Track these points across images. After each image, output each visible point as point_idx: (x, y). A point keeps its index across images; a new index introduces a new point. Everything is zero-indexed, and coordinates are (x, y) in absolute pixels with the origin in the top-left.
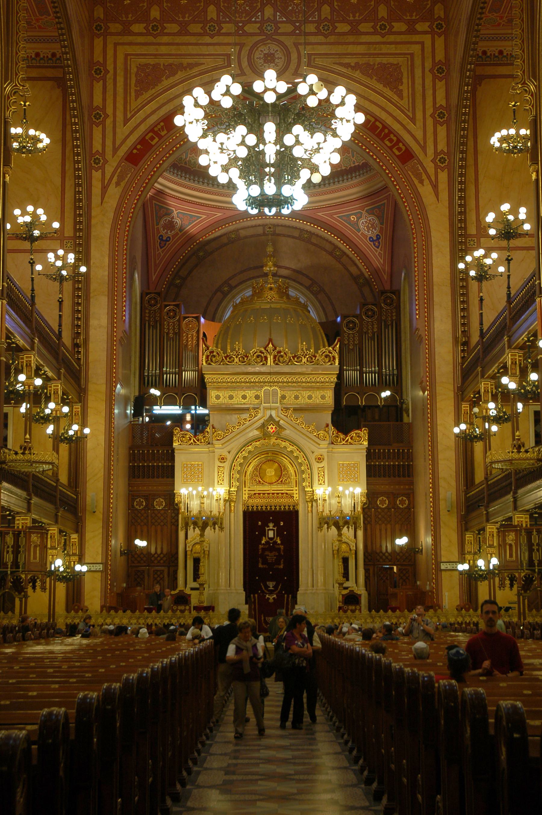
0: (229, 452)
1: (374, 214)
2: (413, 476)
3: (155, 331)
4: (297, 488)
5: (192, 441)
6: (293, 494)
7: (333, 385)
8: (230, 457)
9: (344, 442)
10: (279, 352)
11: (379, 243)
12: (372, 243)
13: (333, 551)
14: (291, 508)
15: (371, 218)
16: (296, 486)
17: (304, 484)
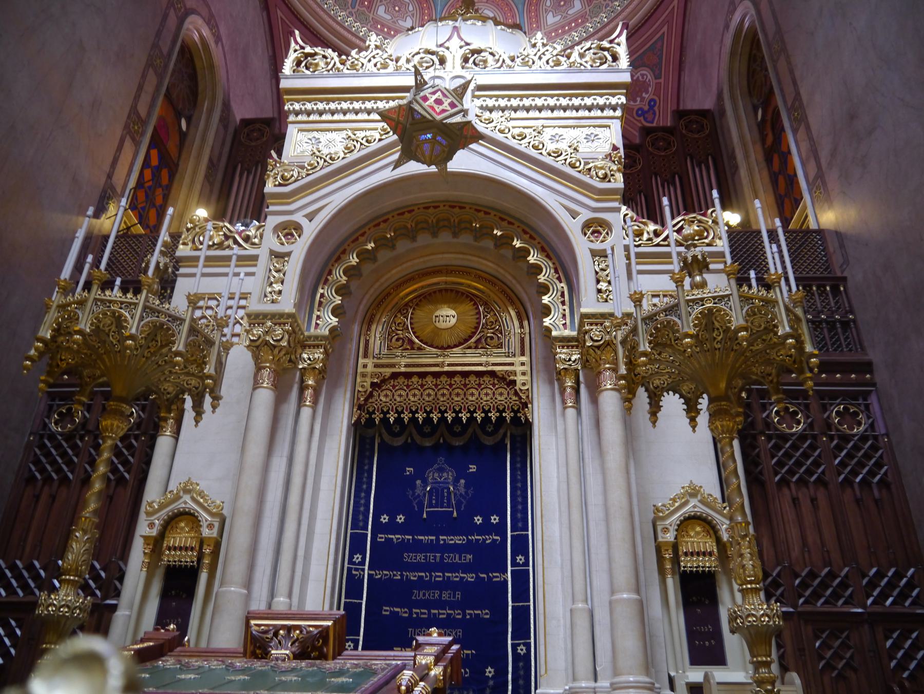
0: (310, 221)
1: (644, 65)
2: (863, 348)
3: (251, 177)
4: (523, 359)
5: (231, 242)
6: (515, 374)
7: (618, 113)
8: (311, 230)
9: (657, 240)
10: (479, 52)
11: (654, 114)
12: (642, 118)
13: (659, 549)
14: (508, 415)
15: (639, 74)
16: (523, 354)
17: (547, 322)
